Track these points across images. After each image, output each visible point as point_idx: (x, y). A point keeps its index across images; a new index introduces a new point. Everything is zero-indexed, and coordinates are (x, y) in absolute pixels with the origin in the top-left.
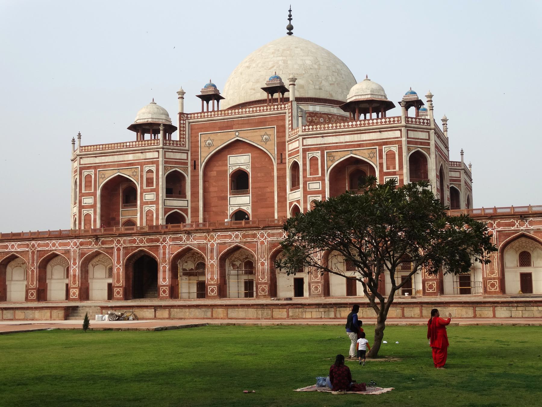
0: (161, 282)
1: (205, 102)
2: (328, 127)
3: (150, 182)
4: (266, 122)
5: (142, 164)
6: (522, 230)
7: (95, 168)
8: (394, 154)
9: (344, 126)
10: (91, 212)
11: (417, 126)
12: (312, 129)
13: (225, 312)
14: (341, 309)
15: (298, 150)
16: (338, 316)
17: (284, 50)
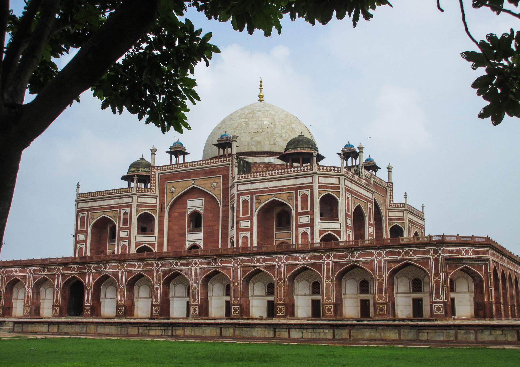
1: (174, 157)
5: (120, 208)
6: (353, 261)
7: (88, 211)
8: (307, 197)
10: (83, 246)
11: (327, 173)
12: (245, 177)
14: (176, 328)
16: (174, 334)
17: (248, 113)
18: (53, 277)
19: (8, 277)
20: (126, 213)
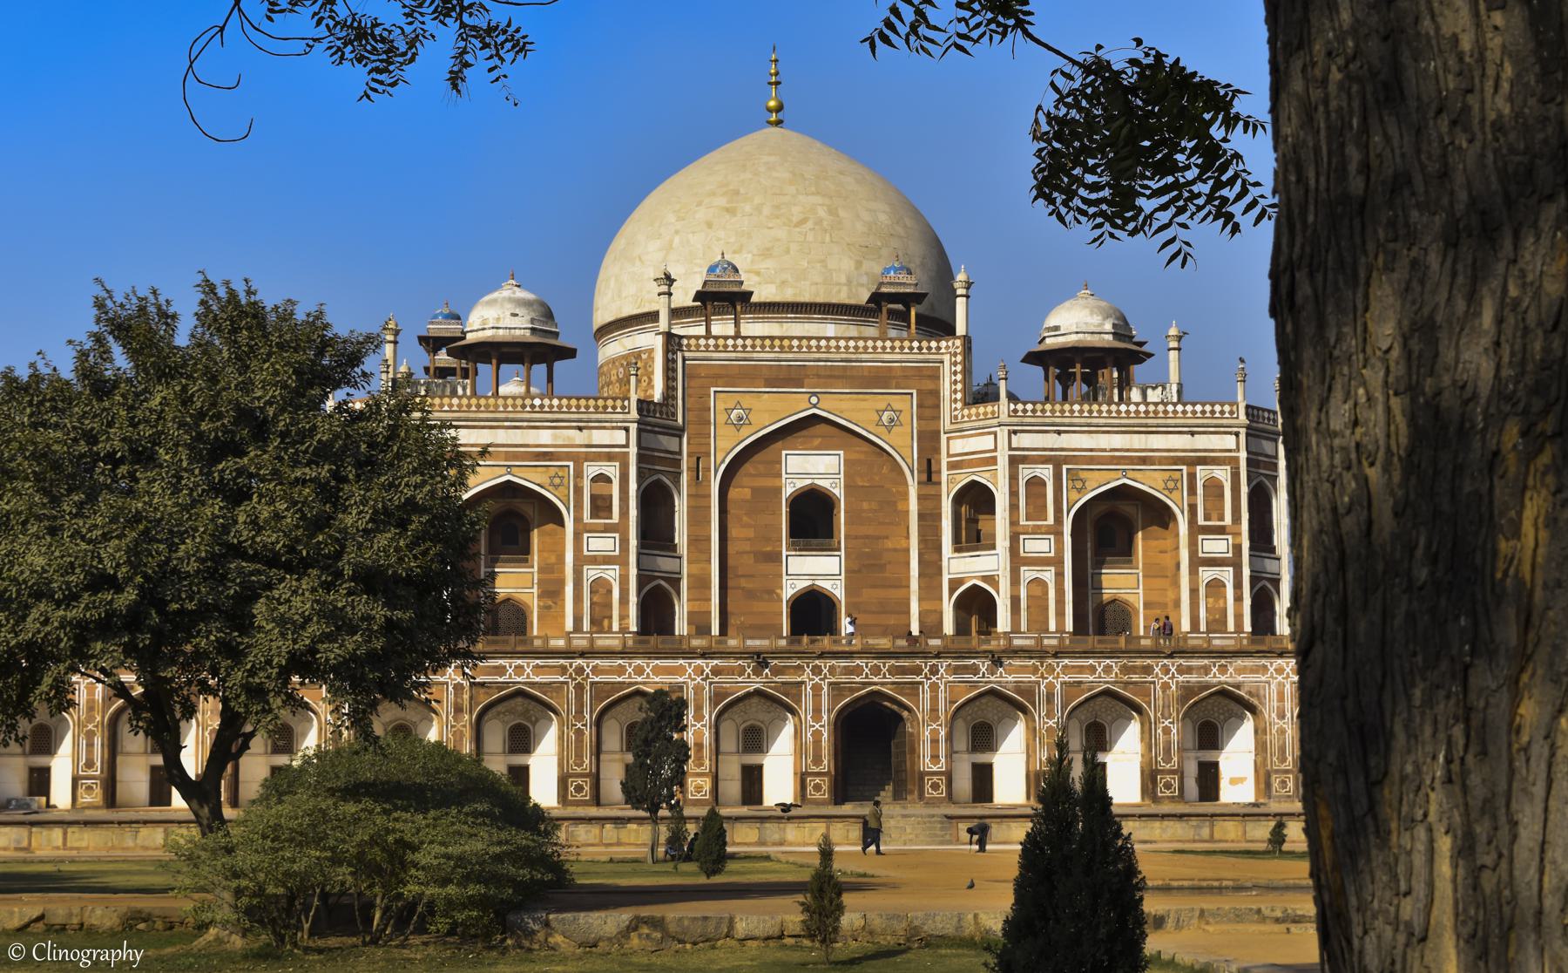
0: (926, 764)
2: (1072, 411)
3: (601, 506)
5: (579, 460)
13: (1240, 829)
15: (995, 458)
18: (794, 691)
19: (600, 690)
20: (602, 478)
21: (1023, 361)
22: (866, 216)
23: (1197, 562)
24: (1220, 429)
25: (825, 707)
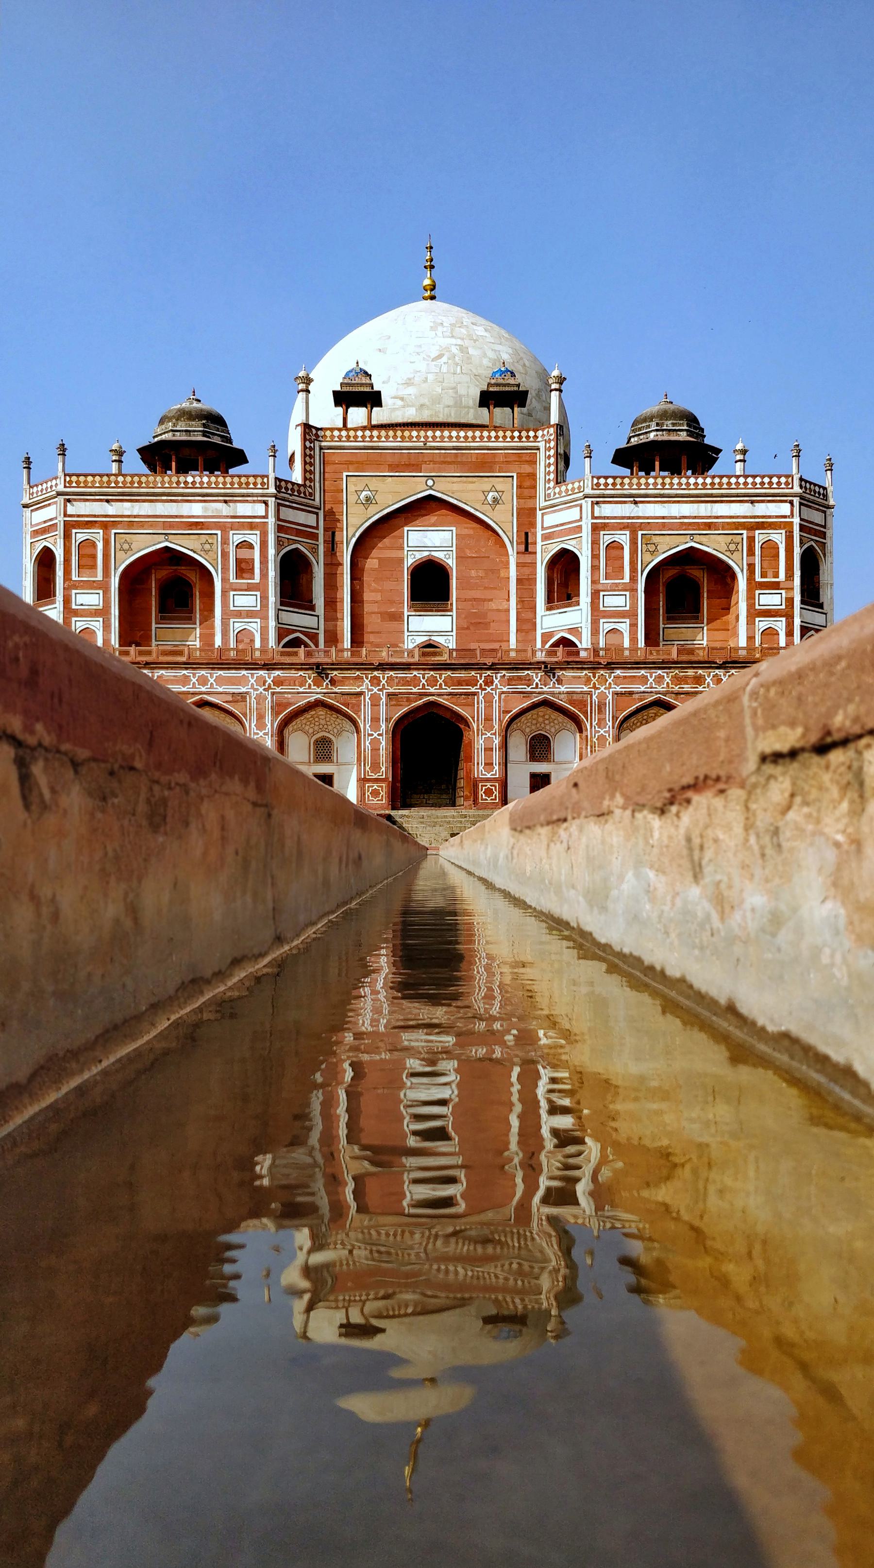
0: (480, 770)
3: (244, 568)
4: (495, 463)
5: (225, 528)
7: (105, 526)
9: (680, 484)
15: (580, 527)
21: (613, 462)
22: (491, 355)
23: (754, 613)
24: (775, 498)
25: (383, 716)
